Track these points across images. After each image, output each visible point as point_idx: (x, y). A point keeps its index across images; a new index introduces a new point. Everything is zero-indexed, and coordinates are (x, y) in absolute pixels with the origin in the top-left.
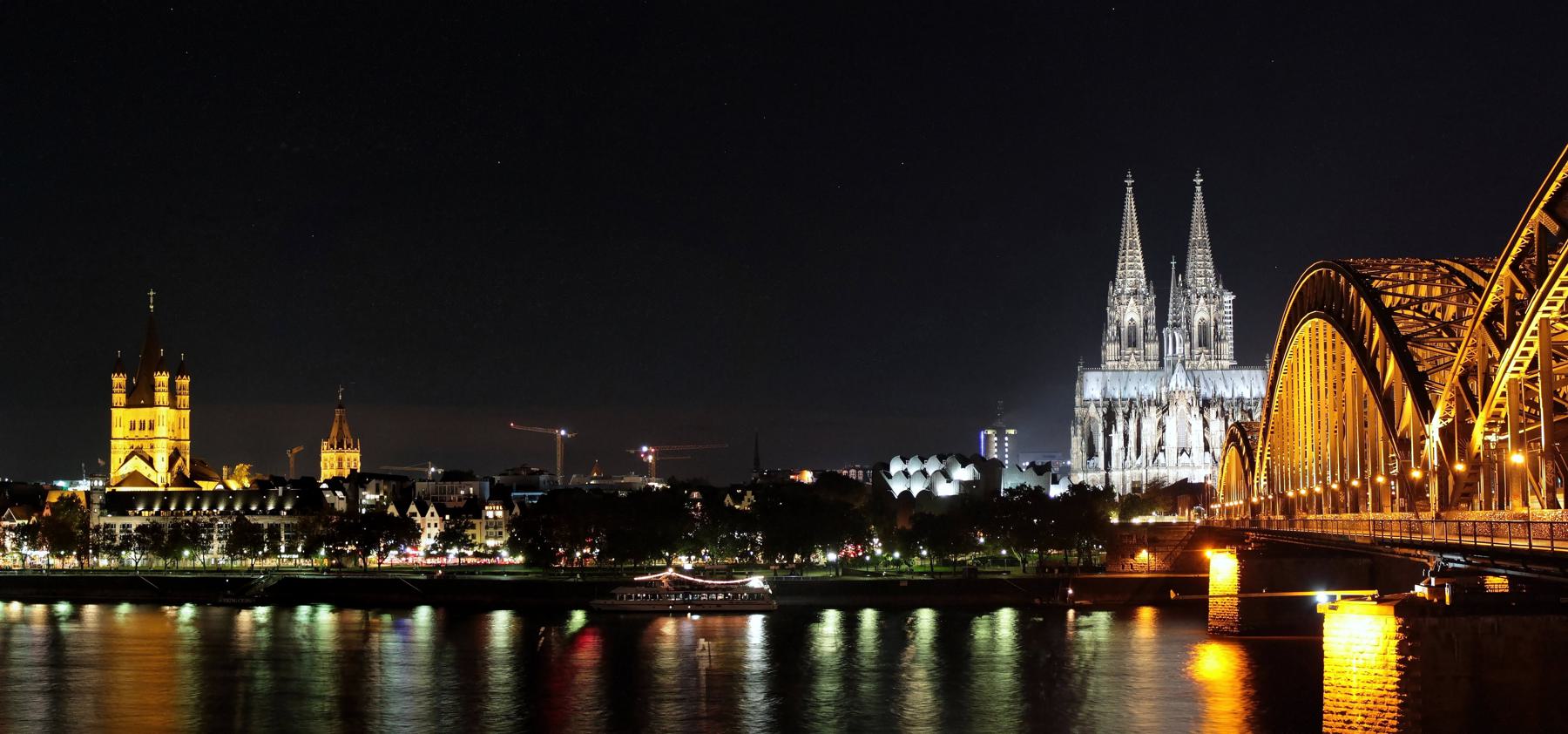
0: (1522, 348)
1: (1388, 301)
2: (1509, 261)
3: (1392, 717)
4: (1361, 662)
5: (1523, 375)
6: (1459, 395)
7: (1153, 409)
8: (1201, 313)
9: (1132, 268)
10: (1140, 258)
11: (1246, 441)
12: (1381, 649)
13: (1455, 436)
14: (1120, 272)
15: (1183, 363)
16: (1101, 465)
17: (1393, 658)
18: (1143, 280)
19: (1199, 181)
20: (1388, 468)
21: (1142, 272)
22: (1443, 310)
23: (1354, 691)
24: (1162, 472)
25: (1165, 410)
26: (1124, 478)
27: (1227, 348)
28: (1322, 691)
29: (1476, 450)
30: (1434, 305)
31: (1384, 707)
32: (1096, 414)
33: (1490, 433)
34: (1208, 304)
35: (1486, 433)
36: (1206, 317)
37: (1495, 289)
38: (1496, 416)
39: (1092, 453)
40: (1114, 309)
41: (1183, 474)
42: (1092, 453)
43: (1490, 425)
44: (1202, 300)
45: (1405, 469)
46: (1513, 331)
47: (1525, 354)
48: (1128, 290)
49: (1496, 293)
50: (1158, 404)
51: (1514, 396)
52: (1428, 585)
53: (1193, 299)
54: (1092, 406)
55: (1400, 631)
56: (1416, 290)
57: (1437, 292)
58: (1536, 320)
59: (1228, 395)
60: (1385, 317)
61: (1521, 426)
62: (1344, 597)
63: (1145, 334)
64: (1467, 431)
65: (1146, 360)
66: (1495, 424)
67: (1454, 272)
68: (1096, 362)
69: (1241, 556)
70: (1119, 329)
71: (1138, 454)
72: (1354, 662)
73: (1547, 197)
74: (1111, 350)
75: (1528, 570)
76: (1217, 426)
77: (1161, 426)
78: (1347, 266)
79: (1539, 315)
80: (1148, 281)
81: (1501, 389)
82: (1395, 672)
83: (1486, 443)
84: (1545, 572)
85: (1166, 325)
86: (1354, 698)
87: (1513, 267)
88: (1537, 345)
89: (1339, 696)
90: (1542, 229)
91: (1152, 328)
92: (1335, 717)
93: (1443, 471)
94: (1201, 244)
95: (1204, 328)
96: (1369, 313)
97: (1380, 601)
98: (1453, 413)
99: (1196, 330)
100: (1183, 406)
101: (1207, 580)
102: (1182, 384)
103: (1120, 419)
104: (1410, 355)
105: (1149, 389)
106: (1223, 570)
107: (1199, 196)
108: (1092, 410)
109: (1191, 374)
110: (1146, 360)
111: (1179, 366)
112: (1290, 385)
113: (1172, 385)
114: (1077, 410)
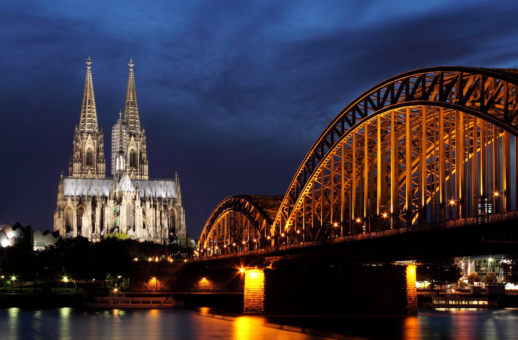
10: (95, 110)
14: (82, 119)
18: (96, 125)
19: (132, 65)
21: (95, 119)
27: (146, 167)
32: (72, 206)
36: (135, 148)
39: (69, 229)
40: (77, 141)
48: (87, 130)
50: (115, 199)
54: (69, 200)
63: (98, 158)
68: (68, 174)
69: (265, 272)
70: (81, 155)
71: (102, 230)
74: (77, 166)
91: (101, 154)
95: (133, 155)
99: (129, 156)
100: (130, 201)
107: (132, 75)
108: (69, 200)
110: (98, 174)
113: (123, 187)
114: (60, 203)
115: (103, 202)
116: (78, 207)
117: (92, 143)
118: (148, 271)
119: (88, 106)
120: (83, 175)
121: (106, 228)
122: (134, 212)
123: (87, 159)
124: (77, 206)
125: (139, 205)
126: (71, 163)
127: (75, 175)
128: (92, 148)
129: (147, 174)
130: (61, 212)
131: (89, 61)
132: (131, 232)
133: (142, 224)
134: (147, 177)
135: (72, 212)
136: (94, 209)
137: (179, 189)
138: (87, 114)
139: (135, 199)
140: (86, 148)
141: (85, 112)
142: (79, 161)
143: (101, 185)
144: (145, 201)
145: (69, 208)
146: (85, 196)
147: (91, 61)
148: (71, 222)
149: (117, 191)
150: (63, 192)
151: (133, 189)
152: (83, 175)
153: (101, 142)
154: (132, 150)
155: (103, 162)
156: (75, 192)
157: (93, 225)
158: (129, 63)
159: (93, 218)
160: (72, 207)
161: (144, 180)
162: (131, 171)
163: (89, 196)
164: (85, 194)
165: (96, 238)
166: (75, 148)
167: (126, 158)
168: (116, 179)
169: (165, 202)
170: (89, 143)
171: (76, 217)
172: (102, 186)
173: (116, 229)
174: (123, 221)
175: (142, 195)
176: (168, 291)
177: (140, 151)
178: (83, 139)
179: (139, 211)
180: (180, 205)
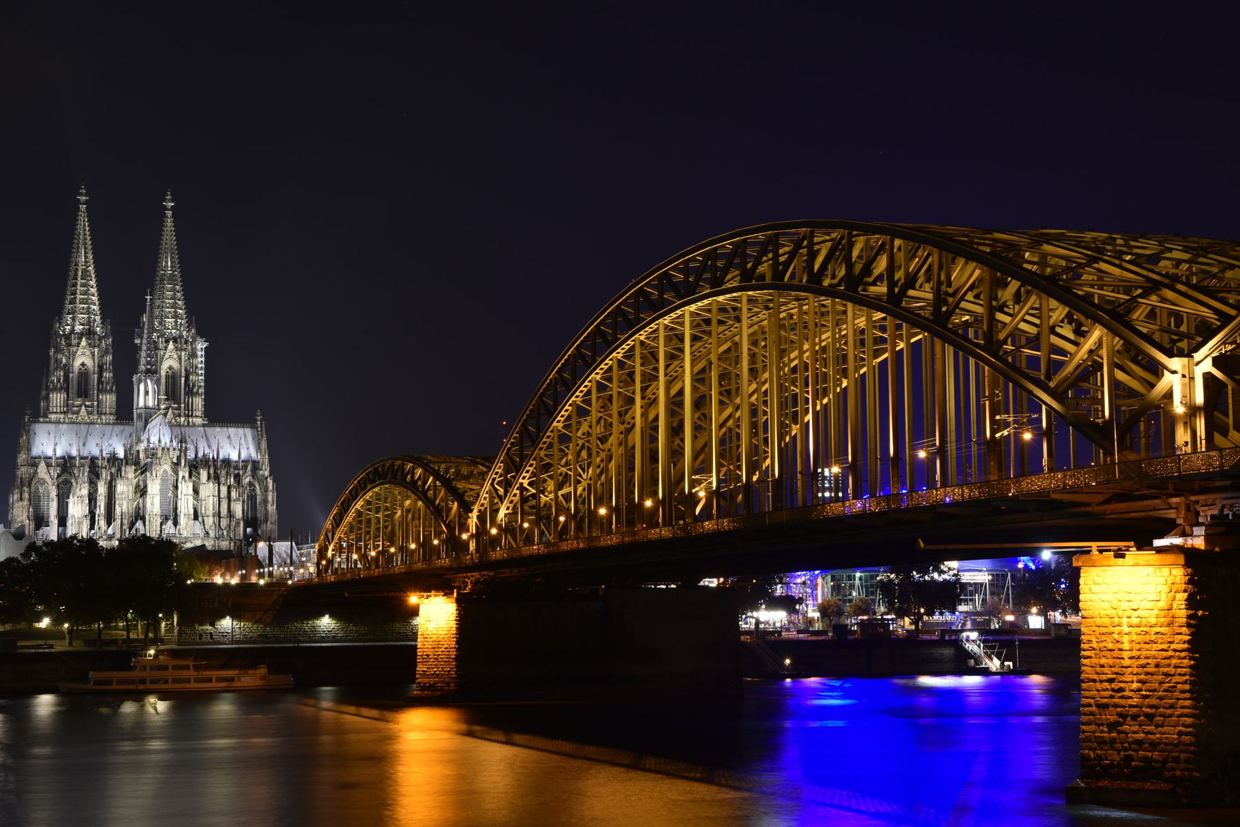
3: (1181, 680)
4: (1135, 621)
7: (130, 472)
12: (1163, 604)
17: (1182, 613)
23: (1126, 654)
25: (143, 469)
27: (198, 402)
31: (1171, 670)
34: (177, 350)
36: (175, 365)
50: (137, 463)
54: (42, 465)
55: (1189, 582)
63: (100, 382)
65: (100, 414)
68: (38, 413)
71: (109, 524)
72: (1125, 621)
74: (57, 399)
77: (142, 491)
82: (1184, 630)
86: (1127, 662)
89: (1103, 661)
91: (107, 375)
92: (1098, 686)
95: (173, 378)
99: (163, 381)
100: (167, 467)
102: (166, 440)
108: (42, 465)
110: (100, 414)
113: (154, 439)
114: (23, 471)
115: (113, 470)
116: (61, 480)
117: (88, 353)
121: (118, 521)
122: (176, 487)
123: (79, 384)
124: (59, 476)
125: (187, 475)
126: (44, 392)
127: (53, 417)
128: (89, 363)
129: (199, 413)
130: (26, 489)
132: (169, 528)
134: (199, 421)
135: (47, 489)
136: (93, 484)
137: (264, 445)
140: (77, 363)
142: (61, 389)
143: (107, 436)
144: (196, 468)
145: (43, 482)
146: (74, 458)
149: (142, 447)
150: (29, 450)
151: (175, 444)
154: (170, 368)
155: (111, 391)
159: (92, 499)
161: (194, 425)
163: (82, 458)
164: (74, 453)
167: (158, 382)
168: (140, 424)
169: (236, 468)
170: (83, 354)
171: (56, 499)
172: (110, 438)
173: (139, 524)
175: (191, 455)
179: (186, 488)
180: (267, 473)
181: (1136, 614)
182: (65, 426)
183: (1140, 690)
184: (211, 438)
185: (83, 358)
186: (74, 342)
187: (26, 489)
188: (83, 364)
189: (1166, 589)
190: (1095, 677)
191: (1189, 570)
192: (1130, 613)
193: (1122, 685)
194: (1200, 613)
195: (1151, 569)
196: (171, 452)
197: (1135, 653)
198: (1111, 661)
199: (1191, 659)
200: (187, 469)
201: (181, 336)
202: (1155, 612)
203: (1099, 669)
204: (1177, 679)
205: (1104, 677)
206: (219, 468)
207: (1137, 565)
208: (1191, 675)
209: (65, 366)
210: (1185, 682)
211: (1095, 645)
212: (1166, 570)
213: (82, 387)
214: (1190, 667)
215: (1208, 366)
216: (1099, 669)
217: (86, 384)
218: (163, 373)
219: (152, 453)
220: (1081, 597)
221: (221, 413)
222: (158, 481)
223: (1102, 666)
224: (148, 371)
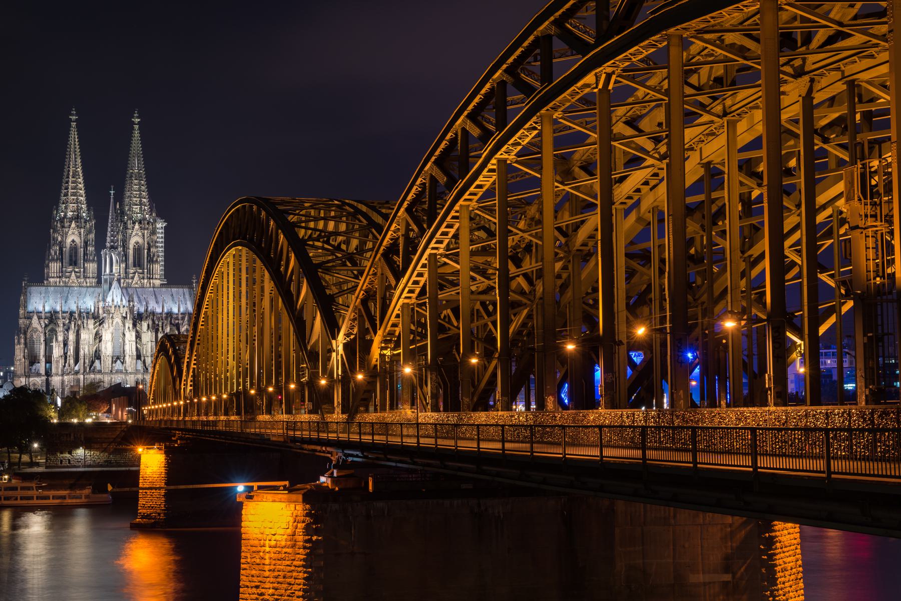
0: (414, 278)
1: (302, 233)
2: (405, 205)
4: (273, 543)
5: (414, 301)
6: (361, 316)
7: (91, 322)
8: (136, 238)
9: (75, 197)
10: (81, 186)
11: (175, 352)
12: (289, 531)
13: (357, 350)
15: (119, 281)
16: (43, 372)
17: (300, 538)
20: (299, 377)
22: (347, 243)
23: (267, 568)
24: (98, 376)
25: (102, 322)
26: (63, 382)
27: (158, 269)
28: (239, 569)
29: (374, 360)
30: (340, 238)
31: (292, 581)
33: (386, 348)
34: (144, 231)
35: (382, 349)
36: (140, 240)
37: (393, 228)
38: (391, 334)
39: (33, 360)
40: (55, 231)
41: (118, 379)
42: (33, 360)
43: (386, 341)
44: (137, 226)
45: (314, 377)
46: (407, 262)
47: (416, 283)
48: (70, 214)
49: (394, 231)
51: (406, 317)
52: (331, 476)
53: (129, 226)
54: (35, 317)
55: (307, 515)
56: (326, 225)
57: (343, 227)
58: (426, 256)
59: (159, 310)
60: (299, 246)
61: (413, 342)
62: (260, 488)
64: (367, 346)
65: (85, 277)
66: (390, 341)
67: (358, 211)
69: (167, 453)
72: (267, 542)
73: (437, 153)
74: (54, 267)
75: (414, 463)
76: (148, 337)
77: (98, 337)
78: (267, 201)
79: (428, 251)
80: (88, 210)
81: (396, 312)
83: (382, 356)
84: (429, 465)
85: (105, 247)
86: (267, 574)
87: (407, 210)
88: (426, 275)
89: (254, 572)
90: (433, 179)
91: (91, 249)
92: (250, 590)
93: (346, 379)
94: (139, 177)
95: (138, 250)
96: (286, 243)
97: (290, 490)
98: (356, 330)
99: (131, 252)
100: (118, 320)
101: (137, 473)
102: (117, 300)
103: (60, 329)
104: (319, 279)
105: (89, 303)
106: (152, 461)
107: (136, 134)
108: (35, 317)
109: (125, 289)
110: (85, 277)
111: (115, 284)
112: (215, 303)
113: (109, 299)
114: (21, 321)
115: (80, 322)
118: (72, 437)
119: (71, 179)
120: (64, 279)
122: (124, 335)
123: (71, 256)
124: (46, 326)
125: (131, 326)
127: (51, 280)
128: (77, 240)
131: (73, 115)
133: (135, 353)
138: (70, 191)
139: (125, 318)
141: (67, 188)
147: (76, 115)
148: (36, 350)
150: (25, 307)
151: (124, 302)
152: (64, 279)
153: (90, 232)
155: (93, 261)
156: (44, 307)
157: (65, 354)
158: (133, 117)
159: (65, 344)
160: (40, 329)
162: (134, 273)
163: (64, 312)
164: (58, 309)
165: (68, 374)
166: (52, 242)
168: (106, 287)
169: (177, 319)
170: (73, 233)
172: (84, 297)
173: (97, 362)
174: (107, 349)
176: (101, 466)
177: (148, 243)
178: (63, 227)
181: (274, 538)
182: (52, 288)
183: (273, 595)
184: (158, 296)
185: (73, 236)
186: (67, 224)
187: (22, 336)
188: (73, 241)
189: (292, 520)
190: (248, 584)
191: (308, 506)
192: (269, 537)
193: (263, 590)
194: (314, 538)
195: (283, 505)
196: (121, 309)
197: (272, 567)
198: (257, 573)
199: (305, 572)
200: (131, 322)
201: (145, 219)
202: (285, 537)
203: (250, 578)
204: (296, 587)
205: (253, 584)
206: (155, 321)
207: (274, 501)
208: (304, 585)
209: (60, 242)
210: (300, 590)
211: (249, 560)
212: (292, 506)
213: (73, 259)
214: (304, 579)
215: (341, 348)
216: (250, 578)
217: (76, 256)
218: (131, 247)
219: (107, 310)
220: (243, 524)
221: (175, 277)
222: (111, 328)
223: (253, 576)
224: (112, 247)
